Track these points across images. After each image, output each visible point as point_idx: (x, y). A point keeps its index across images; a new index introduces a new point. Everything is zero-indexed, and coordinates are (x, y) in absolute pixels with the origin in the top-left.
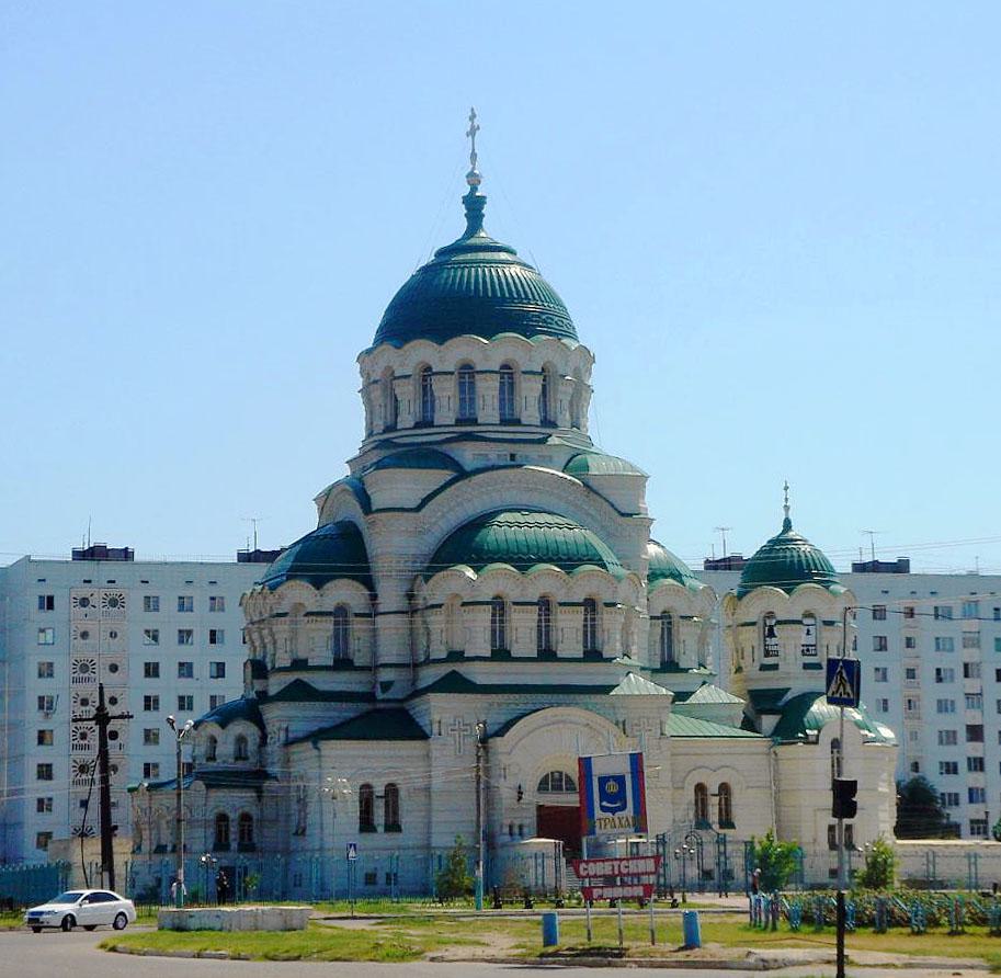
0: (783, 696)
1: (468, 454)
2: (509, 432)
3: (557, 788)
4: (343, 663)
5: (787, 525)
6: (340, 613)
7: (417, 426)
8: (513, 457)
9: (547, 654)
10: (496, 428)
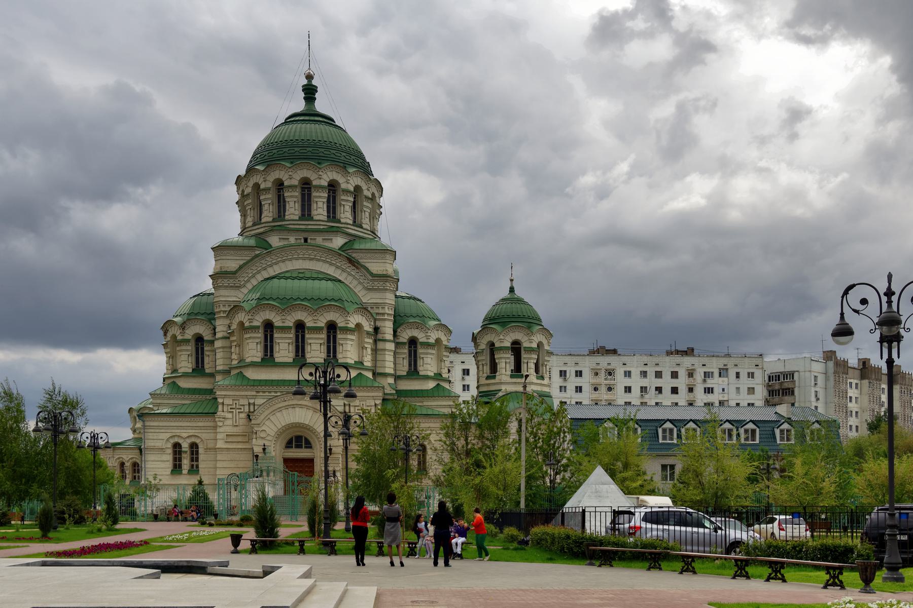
0: (494, 395)
1: (275, 241)
3: (299, 446)
5: (512, 290)
7: (254, 225)
8: (306, 240)
10: (296, 222)
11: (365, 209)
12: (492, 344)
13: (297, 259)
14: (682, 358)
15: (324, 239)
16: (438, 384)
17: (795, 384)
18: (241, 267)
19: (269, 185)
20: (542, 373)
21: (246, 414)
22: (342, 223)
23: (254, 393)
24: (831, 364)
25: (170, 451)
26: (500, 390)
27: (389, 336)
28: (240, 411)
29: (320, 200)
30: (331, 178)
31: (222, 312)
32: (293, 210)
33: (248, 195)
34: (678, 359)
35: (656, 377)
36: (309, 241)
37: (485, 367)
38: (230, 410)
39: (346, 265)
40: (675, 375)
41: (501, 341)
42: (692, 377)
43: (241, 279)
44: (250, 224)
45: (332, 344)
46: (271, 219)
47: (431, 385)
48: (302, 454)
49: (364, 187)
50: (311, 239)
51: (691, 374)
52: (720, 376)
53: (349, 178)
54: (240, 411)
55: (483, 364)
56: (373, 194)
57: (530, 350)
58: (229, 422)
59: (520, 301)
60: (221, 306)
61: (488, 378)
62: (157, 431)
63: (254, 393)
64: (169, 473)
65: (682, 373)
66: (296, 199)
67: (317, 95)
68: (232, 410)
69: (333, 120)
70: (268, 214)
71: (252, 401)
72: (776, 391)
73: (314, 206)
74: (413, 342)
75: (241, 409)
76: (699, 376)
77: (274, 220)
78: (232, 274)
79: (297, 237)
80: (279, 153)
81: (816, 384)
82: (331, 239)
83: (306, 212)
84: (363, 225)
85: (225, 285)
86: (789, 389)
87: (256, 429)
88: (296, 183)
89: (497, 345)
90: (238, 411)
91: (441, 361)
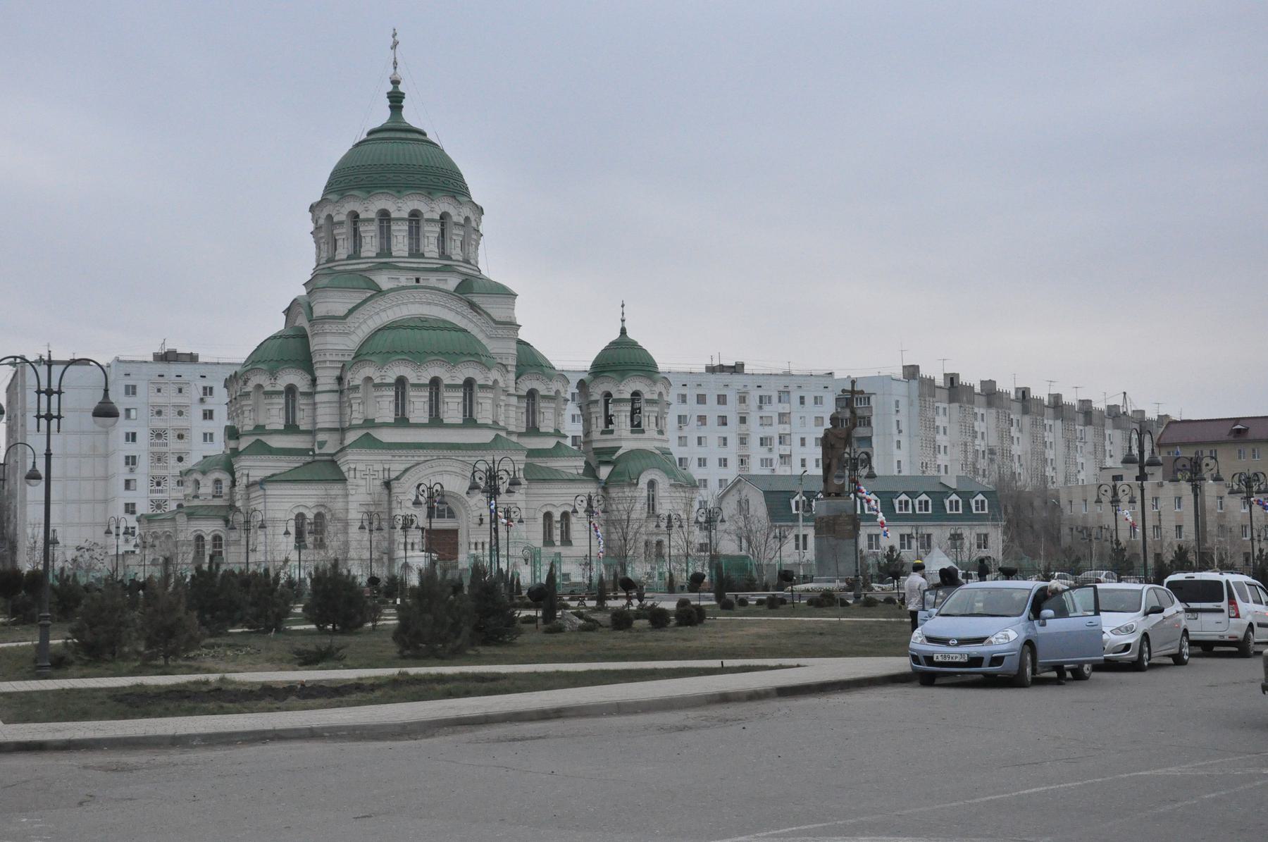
1: (383, 280)
2: (415, 263)
4: (291, 428)
5: (623, 331)
6: (291, 390)
7: (349, 258)
8: (418, 280)
9: (436, 421)
12: (608, 395)
13: (412, 303)
14: (731, 376)
15: (437, 280)
16: (558, 442)
17: (871, 411)
18: (351, 311)
19: (372, 215)
20: (661, 427)
21: (382, 481)
22: (454, 261)
23: (390, 458)
24: (915, 384)
26: (620, 448)
27: (512, 391)
28: (374, 477)
29: (432, 235)
30: (443, 211)
31: (328, 362)
32: (400, 245)
33: (341, 223)
34: (725, 377)
35: (698, 403)
36: (421, 281)
37: (599, 420)
38: (363, 477)
39: (467, 310)
40: (722, 400)
41: (620, 392)
42: (744, 402)
43: (352, 325)
44: (345, 256)
45: (468, 403)
46: (374, 255)
48: (446, 525)
50: (423, 279)
51: (743, 400)
52: (780, 401)
53: (461, 210)
54: (374, 477)
55: (596, 417)
56: (467, 219)
57: (650, 402)
58: (362, 490)
59: (634, 345)
60: (327, 354)
61: (603, 433)
62: (279, 500)
63: (390, 458)
65: (732, 398)
66: (404, 234)
67: (404, 103)
68: (365, 477)
69: (424, 134)
70: (370, 247)
71: (387, 466)
72: (846, 420)
73: (424, 242)
74: (532, 394)
75: (375, 475)
76: (753, 400)
77: (378, 256)
78: (342, 319)
79: (408, 277)
80: (381, 178)
81: (897, 411)
82: (446, 280)
83: (416, 253)
85: (333, 331)
86: (864, 418)
87: (401, 498)
88: (406, 216)
89: (615, 396)
90: (372, 477)
91: (559, 415)
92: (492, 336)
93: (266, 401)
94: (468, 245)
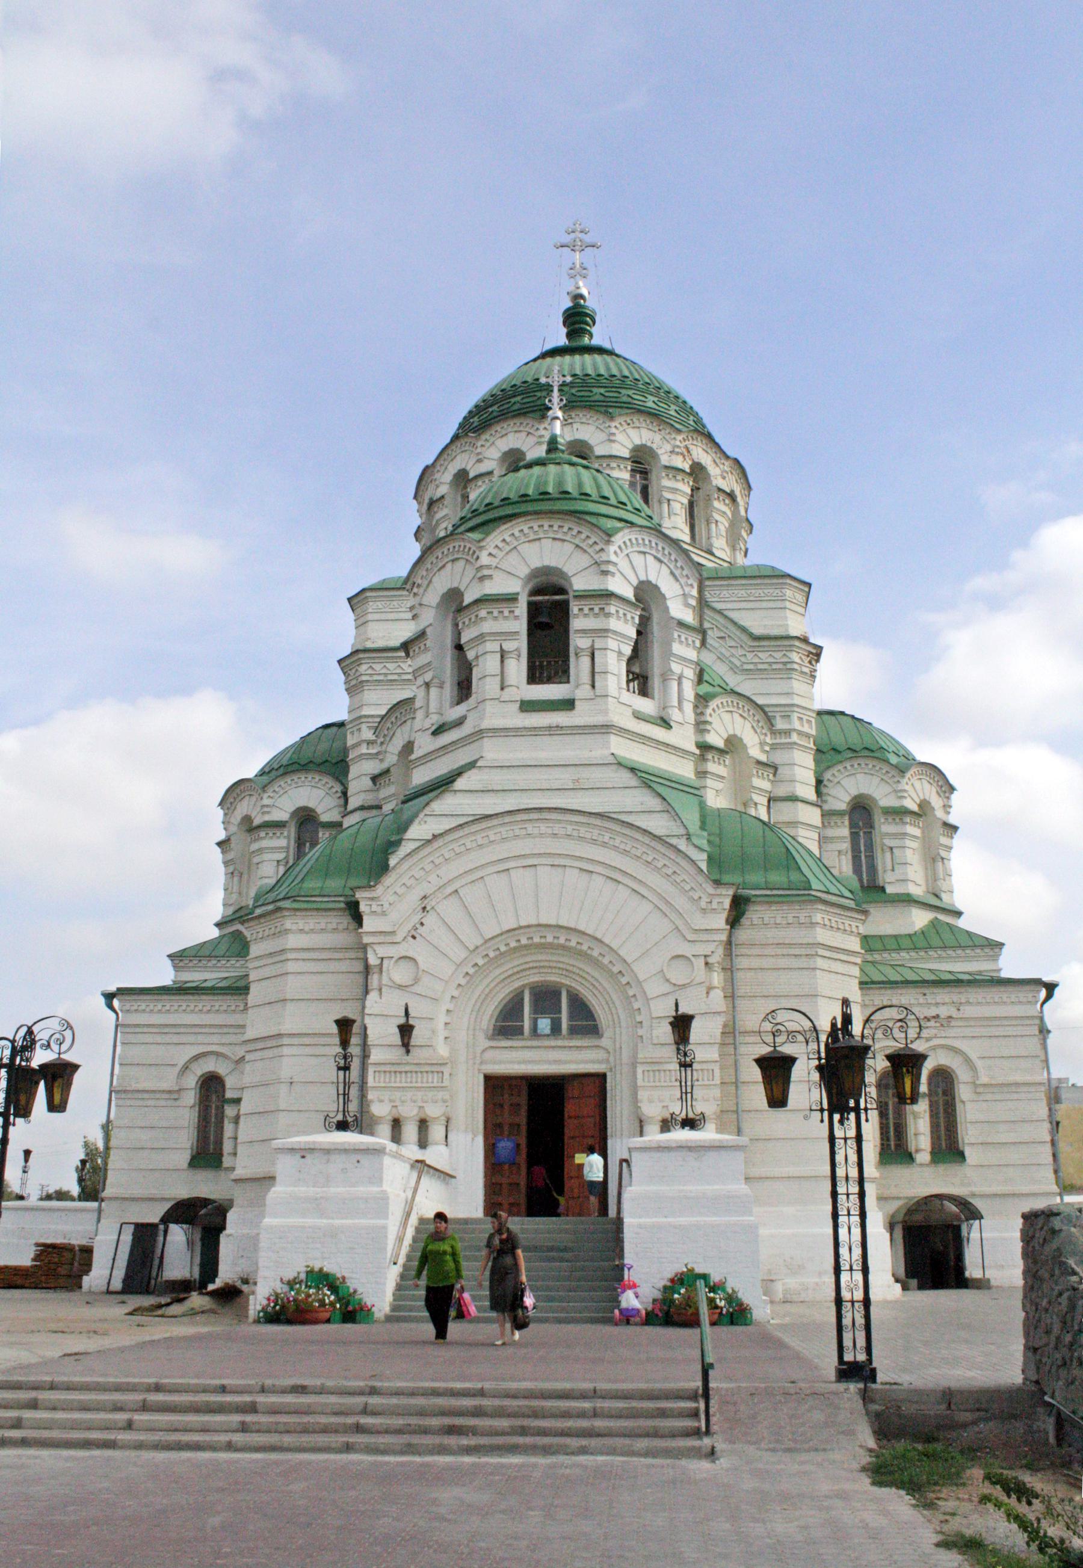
11: (717, 516)
25: (190, 1098)
47: (920, 919)
49: (713, 470)
64: (185, 1165)
84: (715, 551)
92: (746, 667)
93: (255, 846)
94: (708, 523)
